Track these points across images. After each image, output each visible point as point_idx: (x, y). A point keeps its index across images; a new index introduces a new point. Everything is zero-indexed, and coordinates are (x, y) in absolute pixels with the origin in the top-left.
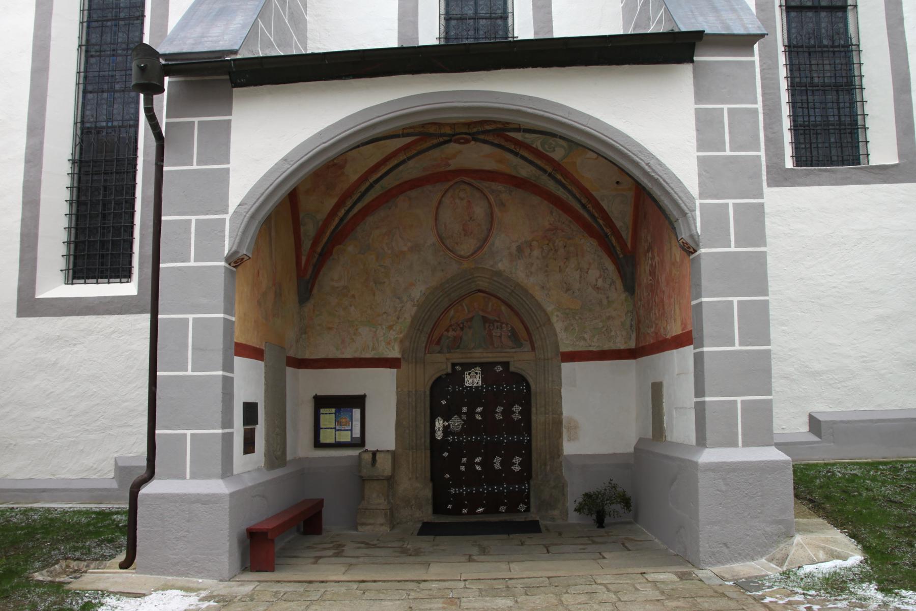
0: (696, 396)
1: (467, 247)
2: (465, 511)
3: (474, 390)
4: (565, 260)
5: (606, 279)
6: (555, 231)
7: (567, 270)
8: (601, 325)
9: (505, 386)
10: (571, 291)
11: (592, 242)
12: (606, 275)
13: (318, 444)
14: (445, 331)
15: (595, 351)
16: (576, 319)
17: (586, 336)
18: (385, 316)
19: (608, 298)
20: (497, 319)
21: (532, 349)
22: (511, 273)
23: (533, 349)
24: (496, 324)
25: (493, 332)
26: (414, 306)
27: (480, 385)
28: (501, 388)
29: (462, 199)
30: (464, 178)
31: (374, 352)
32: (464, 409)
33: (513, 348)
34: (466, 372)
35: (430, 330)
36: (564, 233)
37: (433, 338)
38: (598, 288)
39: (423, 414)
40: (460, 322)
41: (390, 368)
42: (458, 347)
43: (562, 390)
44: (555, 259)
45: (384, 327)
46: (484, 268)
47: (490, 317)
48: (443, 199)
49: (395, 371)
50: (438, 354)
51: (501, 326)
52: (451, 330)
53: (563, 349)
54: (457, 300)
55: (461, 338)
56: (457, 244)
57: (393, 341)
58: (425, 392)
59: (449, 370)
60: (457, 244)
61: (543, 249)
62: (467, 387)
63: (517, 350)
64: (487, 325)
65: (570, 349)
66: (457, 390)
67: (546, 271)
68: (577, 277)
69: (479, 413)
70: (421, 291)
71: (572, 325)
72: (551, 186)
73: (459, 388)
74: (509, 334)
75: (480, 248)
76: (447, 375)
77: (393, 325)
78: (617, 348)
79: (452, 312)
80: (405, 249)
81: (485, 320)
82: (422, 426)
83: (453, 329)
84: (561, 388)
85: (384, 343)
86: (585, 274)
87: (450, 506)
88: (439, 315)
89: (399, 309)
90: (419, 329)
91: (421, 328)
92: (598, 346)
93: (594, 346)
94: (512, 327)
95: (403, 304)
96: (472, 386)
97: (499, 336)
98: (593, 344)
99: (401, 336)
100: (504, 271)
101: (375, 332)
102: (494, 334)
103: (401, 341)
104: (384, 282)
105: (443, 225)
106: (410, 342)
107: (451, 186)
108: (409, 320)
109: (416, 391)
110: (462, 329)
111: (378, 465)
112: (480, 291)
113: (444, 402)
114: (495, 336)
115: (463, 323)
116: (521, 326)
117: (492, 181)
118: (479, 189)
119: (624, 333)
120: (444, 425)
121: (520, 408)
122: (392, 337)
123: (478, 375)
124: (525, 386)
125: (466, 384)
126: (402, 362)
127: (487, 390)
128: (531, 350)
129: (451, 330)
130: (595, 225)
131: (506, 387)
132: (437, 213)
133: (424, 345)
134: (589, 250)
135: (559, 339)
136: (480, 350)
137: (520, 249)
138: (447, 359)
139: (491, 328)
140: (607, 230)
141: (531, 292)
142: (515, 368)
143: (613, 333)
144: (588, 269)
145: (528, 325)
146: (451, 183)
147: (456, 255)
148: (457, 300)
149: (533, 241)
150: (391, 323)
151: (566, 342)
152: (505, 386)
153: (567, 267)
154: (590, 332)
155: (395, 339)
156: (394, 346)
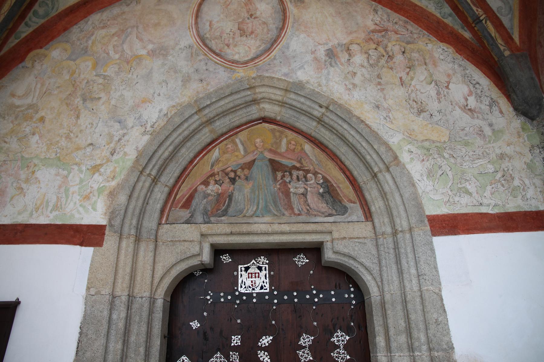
3: (255, 300)
4: (408, 70)
5: (480, 97)
6: (384, 33)
7: (413, 83)
8: (491, 168)
9: (314, 292)
10: (428, 113)
11: (444, 48)
12: (479, 91)
14: (203, 183)
15: (491, 214)
16: (444, 158)
17: (469, 187)
18: (89, 149)
19: (491, 125)
20: (298, 165)
22: (320, 85)
23: (368, 215)
24: (295, 173)
25: (290, 186)
26: (145, 133)
27: (268, 291)
28: (308, 297)
31: (55, 213)
32: (236, 340)
33: (330, 215)
34: (240, 267)
35: (172, 181)
36: (399, 36)
37: (177, 197)
38: (470, 110)
39: (142, 350)
40: (230, 169)
41: (81, 244)
42: (225, 213)
43: (444, 294)
44: (391, 68)
45: (84, 168)
46: (273, 78)
47: (284, 161)
49: (88, 251)
50: (186, 226)
51: (305, 177)
53: (432, 210)
54: (226, 133)
55: (230, 197)
57: (96, 194)
58: (152, 301)
59: (206, 257)
60: (228, 46)
61: (369, 55)
62: (242, 294)
63: (338, 218)
64: (279, 174)
66: (222, 300)
67: (379, 84)
68: (433, 93)
69: (265, 349)
70: (160, 111)
71: (440, 167)
73: (225, 297)
74: (321, 190)
75: (268, 50)
76: (206, 270)
77: (101, 165)
78: (534, 209)
79: (216, 153)
80: (143, 52)
81: (275, 166)
83: (216, 181)
84: (440, 290)
85: (79, 197)
86: (444, 89)
88: (192, 155)
89: (117, 139)
90: (149, 175)
91: (154, 173)
92: (495, 205)
93: (488, 205)
94: (324, 178)
95: (125, 131)
96: (252, 293)
97: (303, 194)
98: (485, 201)
99: (114, 183)
100: (308, 82)
101: (66, 177)
102: (292, 190)
103: (112, 194)
104: (100, 98)
105: (208, 24)
106: (130, 197)
108: (132, 155)
109: (131, 297)
110: (233, 181)
112: (265, 120)
113: (195, 325)
114: (295, 194)
115: (235, 172)
116: (341, 176)
121: (348, 338)
122: (96, 186)
123: (264, 272)
124: (352, 292)
125: (239, 289)
126: (107, 232)
127: (281, 302)
128: (363, 218)
129: (212, 182)
131: (317, 295)
133: (159, 206)
134: (442, 57)
135: (420, 191)
136: (267, 219)
137: (331, 54)
138: (202, 235)
139: (288, 179)
141: (357, 113)
142: (335, 253)
143: (517, 182)
144: (449, 83)
145: (355, 173)
147: (226, 61)
148: (226, 133)
149: (352, 44)
150: (99, 162)
151: (437, 197)
152: (314, 292)
153: (412, 79)
154: (473, 179)
155: (100, 190)
156: (95, 202)
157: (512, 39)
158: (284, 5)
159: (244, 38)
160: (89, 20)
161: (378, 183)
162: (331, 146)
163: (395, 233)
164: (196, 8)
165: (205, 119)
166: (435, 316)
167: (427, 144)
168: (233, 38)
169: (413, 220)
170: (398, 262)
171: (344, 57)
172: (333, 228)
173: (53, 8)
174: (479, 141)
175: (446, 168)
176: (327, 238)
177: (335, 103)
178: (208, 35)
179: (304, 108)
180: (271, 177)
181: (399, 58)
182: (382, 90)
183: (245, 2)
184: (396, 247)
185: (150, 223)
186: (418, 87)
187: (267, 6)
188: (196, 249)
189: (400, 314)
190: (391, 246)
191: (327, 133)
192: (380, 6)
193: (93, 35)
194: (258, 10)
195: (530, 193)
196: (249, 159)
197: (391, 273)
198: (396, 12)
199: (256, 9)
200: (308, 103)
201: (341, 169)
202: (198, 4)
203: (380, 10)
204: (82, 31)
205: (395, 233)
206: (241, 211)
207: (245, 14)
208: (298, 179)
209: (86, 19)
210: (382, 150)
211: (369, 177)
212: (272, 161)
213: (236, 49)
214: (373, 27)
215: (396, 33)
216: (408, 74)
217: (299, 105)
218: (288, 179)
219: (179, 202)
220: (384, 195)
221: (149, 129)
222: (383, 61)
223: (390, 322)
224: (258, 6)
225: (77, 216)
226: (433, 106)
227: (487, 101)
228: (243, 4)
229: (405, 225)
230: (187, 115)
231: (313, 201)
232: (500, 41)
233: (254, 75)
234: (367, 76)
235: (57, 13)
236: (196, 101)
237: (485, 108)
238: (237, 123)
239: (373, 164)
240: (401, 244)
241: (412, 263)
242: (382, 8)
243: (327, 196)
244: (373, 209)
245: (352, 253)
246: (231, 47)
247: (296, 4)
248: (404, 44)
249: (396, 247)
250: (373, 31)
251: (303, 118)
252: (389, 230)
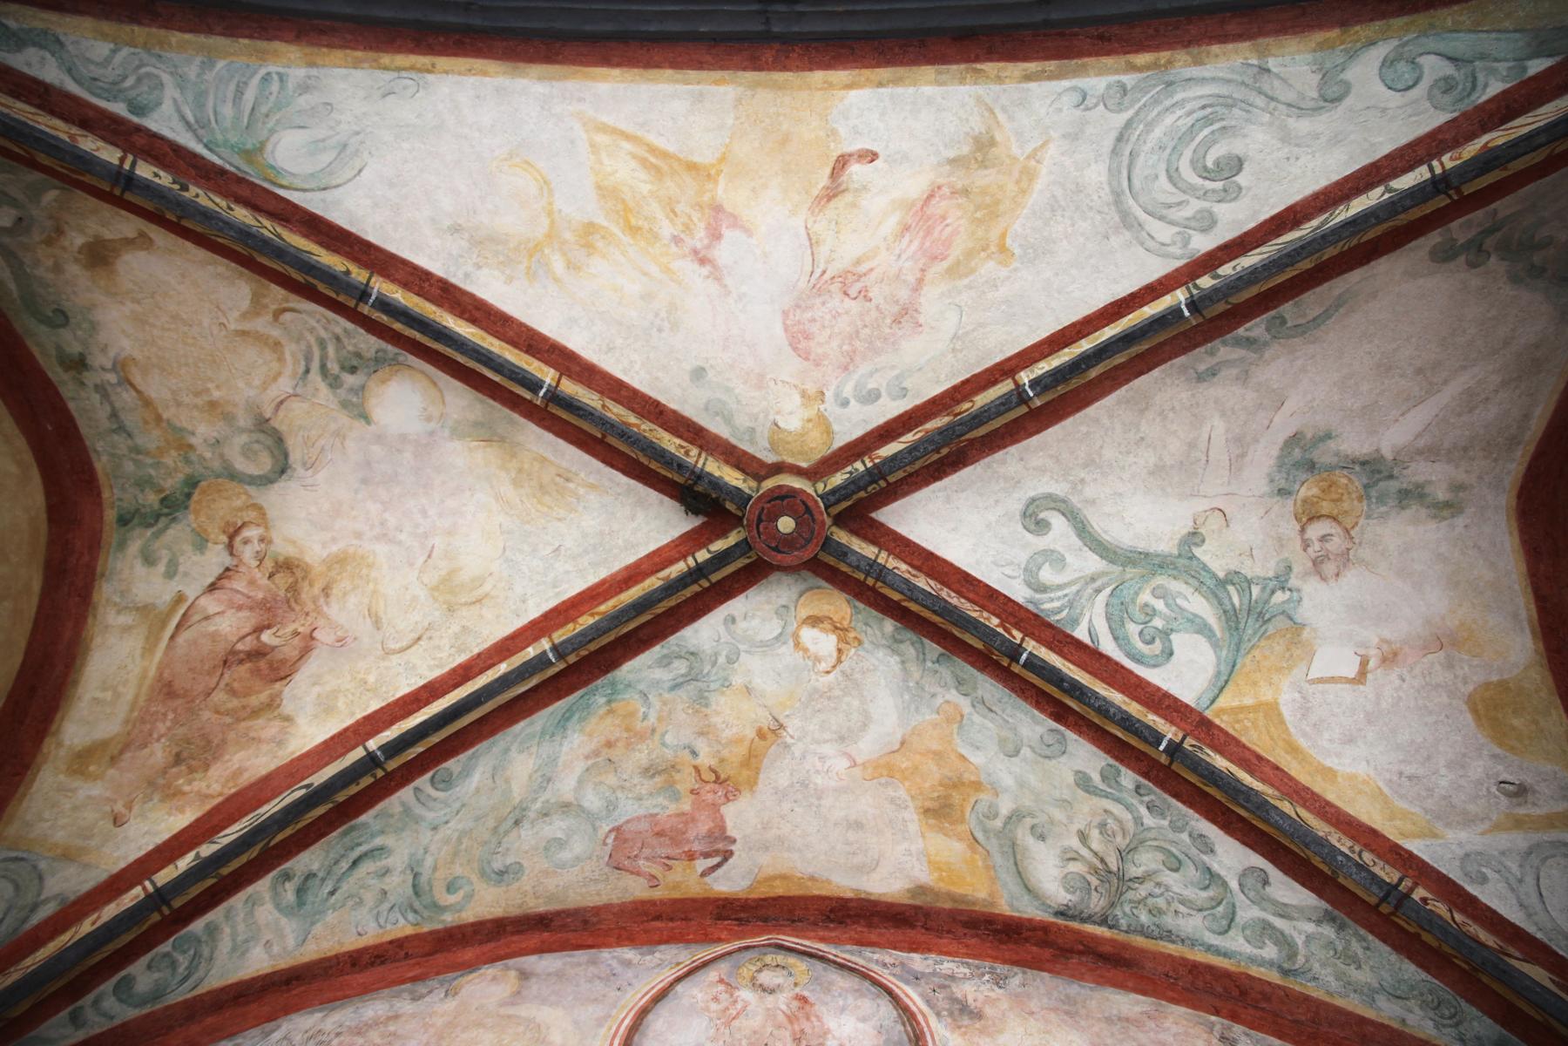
48: (679, 988)
107: (729, 953)
158: (918, 1023)
160: (279, 1027)
164: (627, 1022)
173: (185, 979)
183: (788, 1012)
187: (861, 1025)
194: (830, 1036)
202: (636, 1008)
209: (269, 1026)
228: (781, 1017)
235: (189, 996)
242: (1247, 1035)
247: (955, 1020)
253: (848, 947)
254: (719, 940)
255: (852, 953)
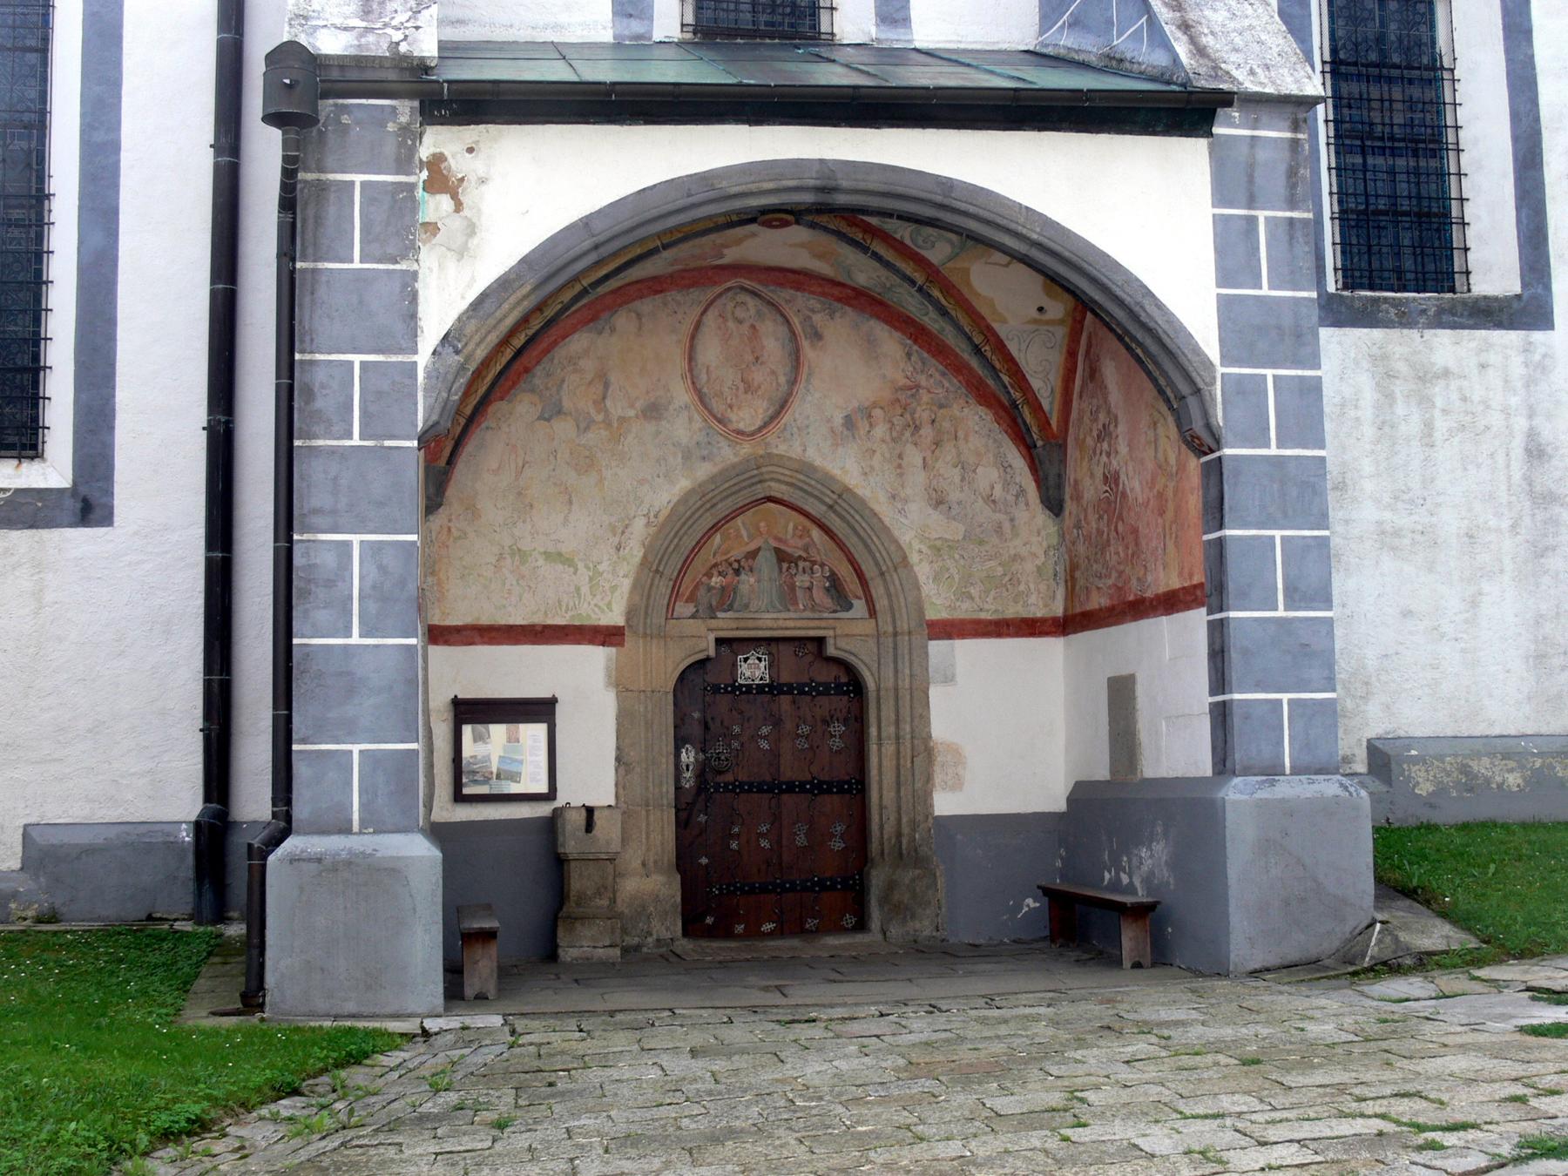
0: (1212, 693)
1: (748, 415)
2: (740, 928)
13: (459, 797)
19: (1012, 520)
20: (804, 555)
21: (871, 616)
23: (872, 612)
24: (801, 564)
26: (648, 524)
29: (740, 322)
30: (742, 280)
33: (835, 611)
38: (994, 501)
49: (612, 651)
52: (715, 573)
53: (931, 615)
55: (735, 590)
56: (731, 407)
59: (712, 652)
60: (731, 407)
62: (741, 685)
64: (785, 565)
65: (944, 615)
68: (957, 479)
69: (765, 738)
72: (910, 302)
81: (781, 556)
82: (664, 760)
87: (709, 920)
90: (657, 571)
92: (996, 611)
94: (831, 570)
98: (986, 606)
108: (638, 554)
110: (737, 572)
111: (597, 831)
117: (798, 289)
118: (773, 305)
119: (1043, 587)
120: (696, 759)
128: (867, 616)
130: (990, 382)
132: (692, 348)
133: (666, 602)
134: (977, 428)
137: (849, 422)
140: (1016, 395)
142: (836, 648)
143: (1022, 587)
145: (863, 568)
146: (718, 289)
153: (937, 460)
157: (1049, 424)
159: (749, 396)
161: (885, 581)
162: (840, 535)
163: (895, 634)
165: (708, 505)
166: (920, 711)
167: (938, 543)
168: (737, 396)
169: (913, 624)
170: (895, 662)
171: (863, 426)
172: (838, 624)
174: (995, 540)
175: (954, 571)
176: (831, 633)
177: (848, 490)
178: (705, 390)
179: (816, 493)
180: (776, 568)
181: (927, 432)
182: (901, 475)
184: (895, 648)
185: (658, 618)
186: (941, 471)
188: (703, 645)
189: (892, 708)
190: (891, 645)
191: (838, 520)
192: (915, 348)
193: (563, 381)
195: (1033, 599)
196: (752, 547)
197: (888, 672)
198: (934, 356)
199: (763, 348)
200: (819, 486)
201: (849, 560)
203: (915, 354)
204: (548, 375)
205: (895, 634)
206: (747, 606)
207: (749, 358)
208: (804, 571)
210: (892, 548)
211: (877, 573)
212: (777, 551)
213: (741, 414)
214: (903, 381)
215: (929, 392)
216: (933, 452)
217: (809, 489)
218: (794, 572)
219: (683, 595)
220: (889, 596)
221: (652, 519)
222: (908, 434)
223: (883, 714)
224: (765, 343)
225: (593, 616)
226: (954, 496)
227: (1014, 490)
229: (906, 627)
230: (691, 503)
231: (819, 596)
232: (1034, 429)
233: (761, 452)
234: (887, 455)
236: (700, 486)
237: (1011, 498)
238: (741, 504)
239: (882, 563)
240: (900, 644)
241: (907, 664)
243: (833, 591)
244: (877, 607)
245: (853, 650)
246: (735, 409)
248: (934, 408)
249: (895, 648)
250: (901, 389)
251: (812, 500)
252: (890, 629)
253: (772, 288)
254: (715, 283)
255: (772, 291)
